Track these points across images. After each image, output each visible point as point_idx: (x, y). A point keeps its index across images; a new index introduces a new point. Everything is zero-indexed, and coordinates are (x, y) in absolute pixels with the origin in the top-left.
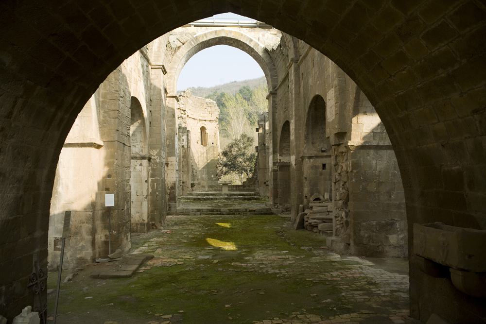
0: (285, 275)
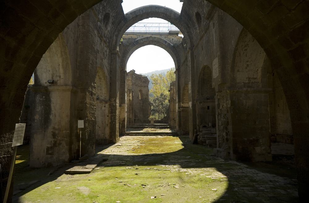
0: (191, 173)
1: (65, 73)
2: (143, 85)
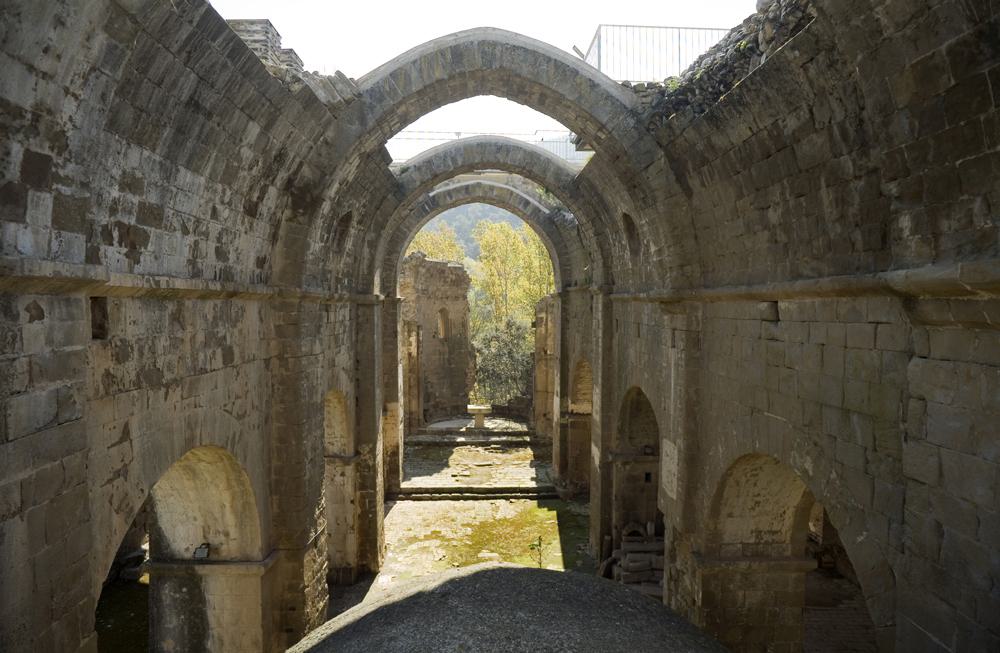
1: (241, 525)
2: (449, 293)
